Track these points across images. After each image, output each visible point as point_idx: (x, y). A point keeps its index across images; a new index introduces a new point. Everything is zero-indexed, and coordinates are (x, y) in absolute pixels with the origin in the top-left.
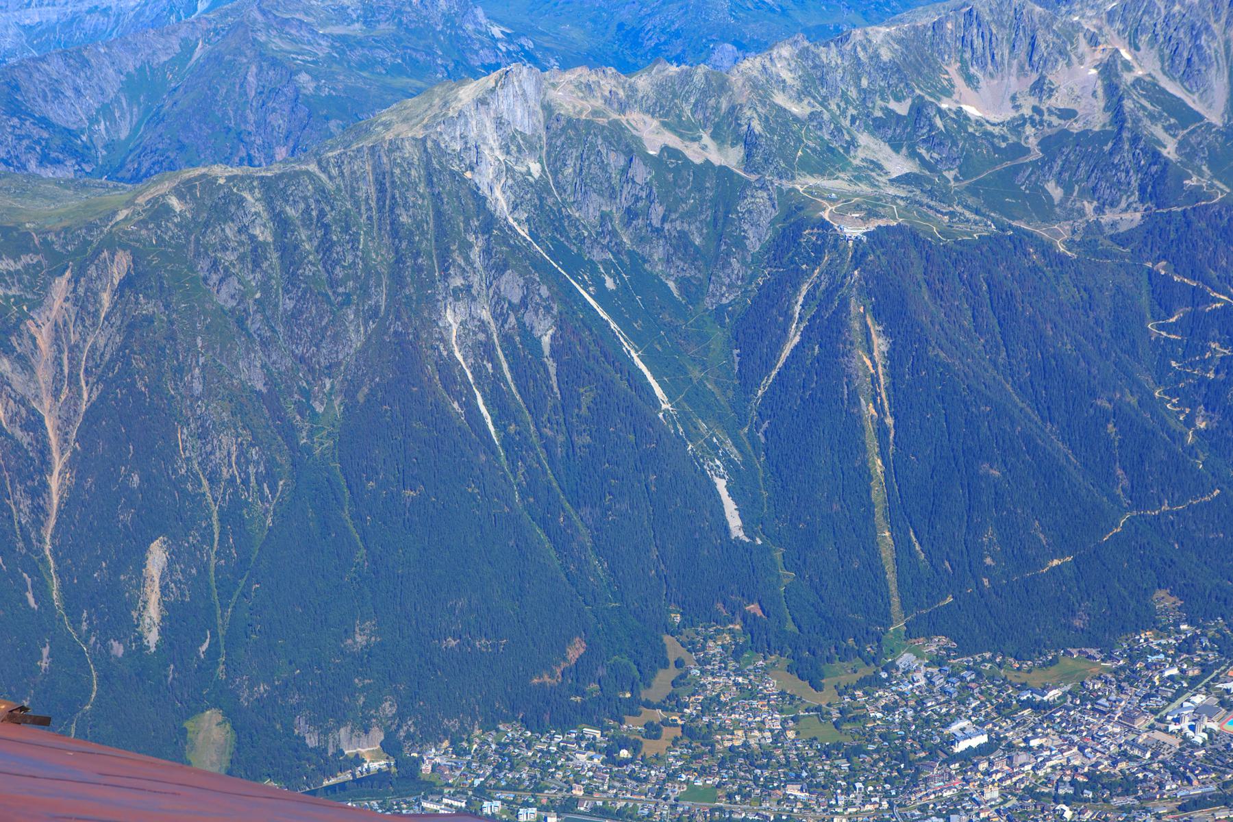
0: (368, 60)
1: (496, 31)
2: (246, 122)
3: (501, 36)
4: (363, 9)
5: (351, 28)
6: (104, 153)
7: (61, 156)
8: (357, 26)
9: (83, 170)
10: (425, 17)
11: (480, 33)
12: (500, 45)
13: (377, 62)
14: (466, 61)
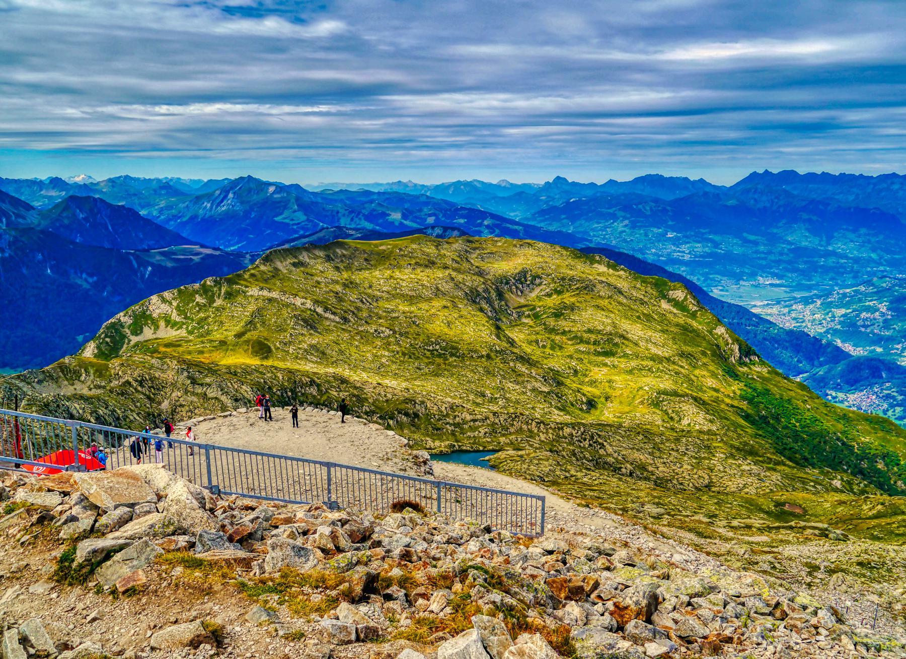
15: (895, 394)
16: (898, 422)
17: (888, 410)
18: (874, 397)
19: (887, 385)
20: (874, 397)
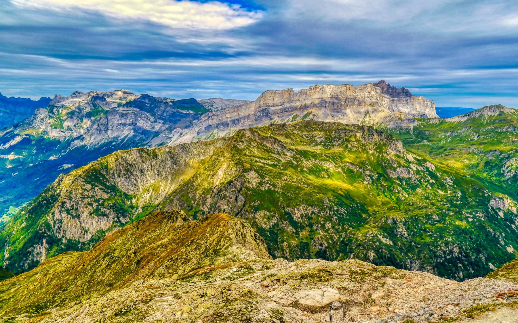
0: (317, 168)
1: (410, 157)
2: (204, 204)
3: (413, 160)
4: (326, 138)
5: (315, 148)
6: (141, 211)
7: (107, 211)
8: (319, 147)
9: (120, 222)
10: (363, 145)
11: (399, 157)
12: (411, 166)
13: (323, 170)
14: (387, 174)
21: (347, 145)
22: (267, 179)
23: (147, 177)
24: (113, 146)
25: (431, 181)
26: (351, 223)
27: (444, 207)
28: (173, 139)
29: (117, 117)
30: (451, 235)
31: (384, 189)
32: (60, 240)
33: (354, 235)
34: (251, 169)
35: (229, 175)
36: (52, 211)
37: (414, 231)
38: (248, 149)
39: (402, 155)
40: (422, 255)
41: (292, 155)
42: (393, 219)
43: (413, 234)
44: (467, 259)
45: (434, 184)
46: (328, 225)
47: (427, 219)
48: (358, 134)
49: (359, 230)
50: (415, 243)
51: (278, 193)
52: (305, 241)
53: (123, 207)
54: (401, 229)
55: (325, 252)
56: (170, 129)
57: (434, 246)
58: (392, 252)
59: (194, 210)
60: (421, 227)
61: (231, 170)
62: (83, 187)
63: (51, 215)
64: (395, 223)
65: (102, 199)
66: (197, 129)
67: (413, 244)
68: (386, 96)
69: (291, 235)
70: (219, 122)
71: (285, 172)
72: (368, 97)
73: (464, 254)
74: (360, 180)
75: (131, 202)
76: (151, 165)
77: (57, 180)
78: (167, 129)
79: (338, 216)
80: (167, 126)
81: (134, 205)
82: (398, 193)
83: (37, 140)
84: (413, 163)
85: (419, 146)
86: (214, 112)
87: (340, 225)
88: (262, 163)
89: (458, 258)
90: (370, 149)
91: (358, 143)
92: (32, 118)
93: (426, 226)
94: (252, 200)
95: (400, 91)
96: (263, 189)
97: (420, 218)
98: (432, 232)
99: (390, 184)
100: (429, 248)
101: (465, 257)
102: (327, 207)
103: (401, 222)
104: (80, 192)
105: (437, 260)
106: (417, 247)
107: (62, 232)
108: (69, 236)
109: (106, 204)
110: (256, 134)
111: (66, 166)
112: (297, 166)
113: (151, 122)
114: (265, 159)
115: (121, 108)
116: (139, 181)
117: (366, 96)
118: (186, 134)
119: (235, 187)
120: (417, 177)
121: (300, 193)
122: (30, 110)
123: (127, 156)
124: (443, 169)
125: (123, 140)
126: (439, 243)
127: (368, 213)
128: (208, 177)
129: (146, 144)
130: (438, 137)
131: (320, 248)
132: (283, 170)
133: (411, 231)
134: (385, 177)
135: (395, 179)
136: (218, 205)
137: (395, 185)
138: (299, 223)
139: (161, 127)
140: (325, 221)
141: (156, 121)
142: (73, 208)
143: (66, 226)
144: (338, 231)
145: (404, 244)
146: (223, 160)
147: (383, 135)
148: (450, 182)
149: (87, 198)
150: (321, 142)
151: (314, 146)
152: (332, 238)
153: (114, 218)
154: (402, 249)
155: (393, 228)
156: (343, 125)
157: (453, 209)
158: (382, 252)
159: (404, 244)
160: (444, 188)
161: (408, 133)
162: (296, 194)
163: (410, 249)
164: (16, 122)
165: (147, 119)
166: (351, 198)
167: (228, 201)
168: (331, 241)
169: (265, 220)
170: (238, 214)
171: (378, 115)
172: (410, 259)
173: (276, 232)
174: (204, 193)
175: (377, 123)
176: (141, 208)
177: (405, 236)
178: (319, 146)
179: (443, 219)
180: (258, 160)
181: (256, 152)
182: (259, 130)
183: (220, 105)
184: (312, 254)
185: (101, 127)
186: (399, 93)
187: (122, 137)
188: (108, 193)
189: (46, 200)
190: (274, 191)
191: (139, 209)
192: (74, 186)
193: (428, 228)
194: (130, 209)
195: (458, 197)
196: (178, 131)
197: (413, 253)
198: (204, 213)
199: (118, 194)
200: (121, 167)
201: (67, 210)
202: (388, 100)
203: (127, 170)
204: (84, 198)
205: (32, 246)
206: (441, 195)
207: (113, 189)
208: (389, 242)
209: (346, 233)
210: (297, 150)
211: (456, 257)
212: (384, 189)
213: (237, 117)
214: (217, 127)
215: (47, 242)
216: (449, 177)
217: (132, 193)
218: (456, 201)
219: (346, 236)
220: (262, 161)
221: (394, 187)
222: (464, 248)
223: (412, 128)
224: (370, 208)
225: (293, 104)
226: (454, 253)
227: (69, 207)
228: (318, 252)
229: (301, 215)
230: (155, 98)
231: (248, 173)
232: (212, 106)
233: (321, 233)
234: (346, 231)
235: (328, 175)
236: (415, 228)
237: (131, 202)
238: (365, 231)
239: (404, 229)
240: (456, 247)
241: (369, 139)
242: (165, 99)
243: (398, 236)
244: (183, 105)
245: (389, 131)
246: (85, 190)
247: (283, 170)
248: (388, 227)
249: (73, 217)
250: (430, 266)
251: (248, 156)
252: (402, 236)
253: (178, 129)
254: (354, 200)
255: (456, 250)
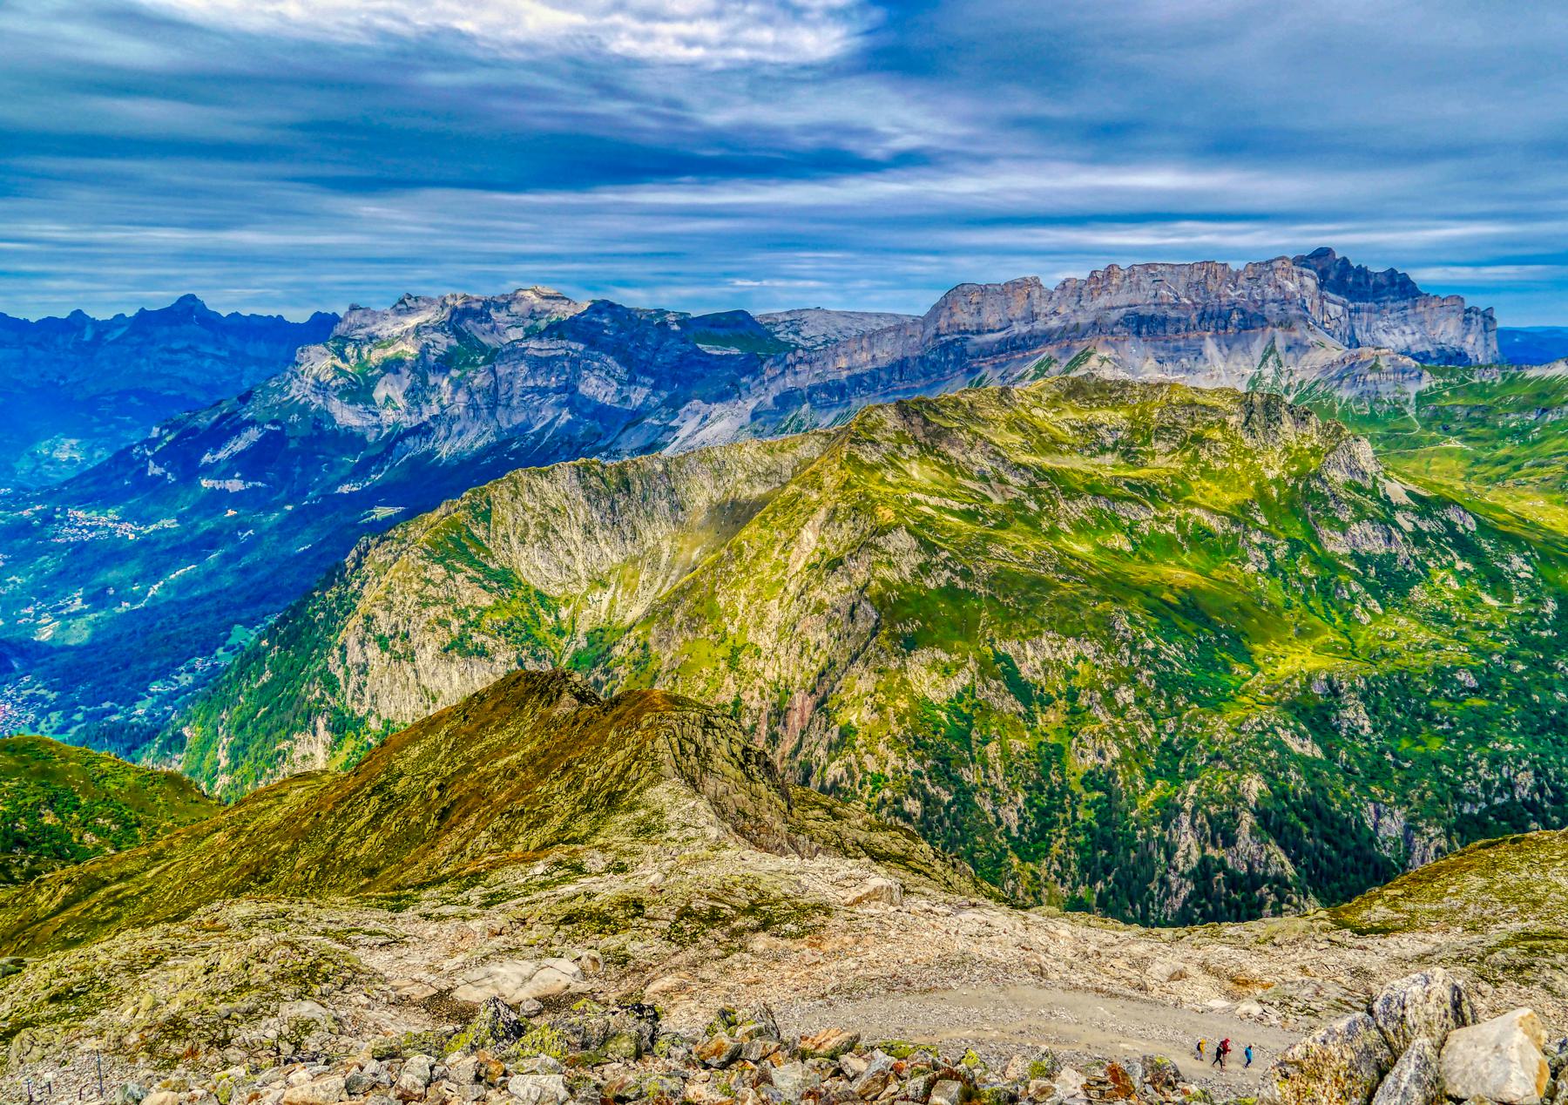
1: (1396, 491)
3: (1405, 500)
5: (1096, 461)
8: (1109, 458)
10: (1248, 452)
11: (1359, 489)
12: (1399, 517)
14: (1318, 543)
15: (43, 692)
16: (58, 738)
17: (37, 723)
18: (8, 707)
19: (26, 679)
20: (8, 707)
21: (1196, 452)
22: (945, 554)
23: (602, 544)
24: (513, 453)
25: (1460, 566)
26: (1196, 691)
27: (1497, 646)
28: (682, 434)
29: (523, 368)
30: (1514, 735)
31: (1308, 590)
32: (361, 721)
33: (1202, 725)
34: (897, 526)
35: (833, 541)
36: (340, 641)
37: (1394, 720)
38: (892, 464)
39: (1368, 485)
40: (1414, 794)
41: (1026, 484)
42: (1329, 681)
43: (1391, 728)
44: (1558, 808)
45: (1470, 574)
46: (1125, 695)
47: (1437, 682)
48: (1233, 420)
49: (1220, 710)
50: (1394, 755)
51: (978, 598)
52: (1052, 739)
53: (534, 631)
54: (1351, 710)
55: (1111, 774)
56: (674, 404)
57: (1454, 765)
58: (1318, 781)
59: (730, 642)
60: (1417, 705)
61: (840, 526)
62: (423, 574)
63: (336, 652)
64: (1335, 692)
65: (475, 609)
66: (752, 404)
67: (1389, 757)
68: (1332, 296)
69: (1013, 723)
70: (816, 381)
71: (1000, 533)
72: (1274, 301)
73: (1549, 792)
74: (1233, 561)
75: (557, 617)
76: (614, 512)
77: (354, 553)
78: (665, 403)
79: (1156, 670)
80: (664, 394)
81: (565, 626)
82: (1352, 601)
83: (302, 438)
84: (1405, 508)
85: (1433, 454)
86: (800, 353)
87: (1160, 695)
88: (932, 507)
89: (1531, 806)
90: (1268, 466)
91: (1233, 447)
92: (288, 375)
93: (1434, 703)
94: (899, 616)
95: (1383, 280)
96: (932, 586)
97: (1416, 679)
98: (1452, 724)
99: (1328, 573)
100: (1438, 771)
101: (1553, 801)
102: (1124, 640)
103: (1353, 689)
104: (415, 587)
105: (1461, 808)
106: (1400, 768)
107: (367, 699)
108: (387, 709)
109: (487, 622)
110: (916, 420)
111: (381, 512)
112: (1039, 515)
113: (620, 382)
114: (942, 495)
115: (533, 344)
116: (580, 557)
117: (1270, 297)
118: (720, 417)
119: (850, 576)
120: (1416, 552)
121: (1044, 599)
122: (283, 351)
123: (545, 484)
124: (1502, 528)
125: (540, 435)
126: (1472, 758)
127: (1251, 662)
128: (772, 548)
129: (605, 449)
130: (1495, 427)
131: (1099, 761)
132: (995, 527)
133: (1386, 719)
134: (1309, 549)
135: (1343, 557)
136: (798, 630)
137: (1343, 578)
138: (1035, 686)
139: (647, 398)
140: (1116, 683)
141: (632, 381)
142: (397, 633)
143: (378, 686)
144: (1153, 715)
145: (1358, 757)
146: (815, 497)
147: (1312, 420)
148: (1521, 569)
149: (435, 604)
150: (1116, 443)
151: (1092, 456)
152: (1133, 732)
153: (508, 663)
154: (1350, 771)
155: (1329, 707)
156: (1186, 391)
157: (1527, 652)
158: (1286, 780)
159: (1358, 757)
160: (1500, 588)
161: (1400, 412)
162: (1032, 600)
163: (1378, 772)
164: (246, 385)
165: (608, 373)
166: (1203, 615)
167: (830, 619)
168: (1133, 741)
169: (935, 676)
170: (856, 657)
171: (1305, 358)
172: (1376, 803)
173: (966, 711)
174: (759, 594)
175: (1301, 383)
176: (586, 634)
177: (1363, 733)
178: (1109, 456)
179: (1490, 685)
180: (920, 497)
181: (915, 474)
182: (928, 407)
183: (823, 330)
184: (1072, 779)
185: (477, 397)
186: (1378, 288)
187: (537, 428)
188: (491, 591)
189: (324, 609)
190: (966, 590)
191: (580, 637)
192: (397, 570)
193: (1438, 710)
194: (554, 636)
195: (1546, 615)
196: (696, 408)
197: (1387, 783)
198: (758, 652)
199: (519, 594)
200: (527, 517)
201: (381, 638)
202: (1339, 308)
203: (545, 527)
204: (425, 605)
205: (287, 737)
206: (1490, 608)
207: (505, 579)
208: (1312, 750)
209: (1180, 720)
210: (1040, 469)
211: (1524, 802)
212: (1308, 590)
213: (870, 367)
214: (810, 396)
215: (327, 728)
216: (1520, 552)
217: (560, 591)
218: (1536, 627)
219: (1178, 728)
220: (932, 501)
221: (1338, 584)
222: (1551, 773)
223: (1413, 397)
224: (1258, 647)
225: (1039, 326)
226: (1519, 789)
227: (386, 630)
228: (1091, 773)
229: (1043, 663)
230: (630, 310)
231: (889, 536)
232: (797, 333)
233: (1102, 717)
234: (1179, 715)
235: (1134, 544)
236: (1399, 710)
237: (557, 617)
238: (1241, 714)
239: (1362, 711)
240: (1525, 769)
241: (1265, 434)
242: (661, 312)
243: (1343, 733)
244: (714, 331)
245: (1338, 408)
246: (428, 581)
247: (995, 527)
248: (1311, 704)
249: (398, 658)
250: (1437, 826)
251: (890, 484)
252: (1356, 732)
253: (696, 404)
254: (1209, 621)
255: (1526, 780)
